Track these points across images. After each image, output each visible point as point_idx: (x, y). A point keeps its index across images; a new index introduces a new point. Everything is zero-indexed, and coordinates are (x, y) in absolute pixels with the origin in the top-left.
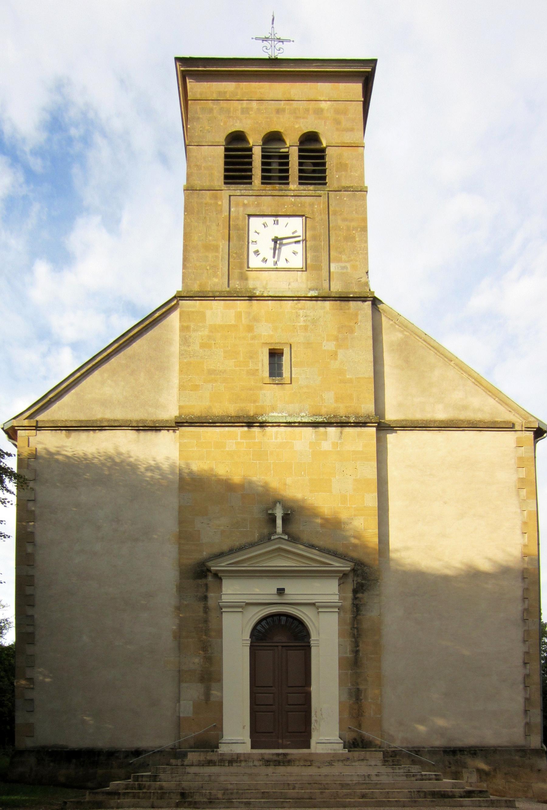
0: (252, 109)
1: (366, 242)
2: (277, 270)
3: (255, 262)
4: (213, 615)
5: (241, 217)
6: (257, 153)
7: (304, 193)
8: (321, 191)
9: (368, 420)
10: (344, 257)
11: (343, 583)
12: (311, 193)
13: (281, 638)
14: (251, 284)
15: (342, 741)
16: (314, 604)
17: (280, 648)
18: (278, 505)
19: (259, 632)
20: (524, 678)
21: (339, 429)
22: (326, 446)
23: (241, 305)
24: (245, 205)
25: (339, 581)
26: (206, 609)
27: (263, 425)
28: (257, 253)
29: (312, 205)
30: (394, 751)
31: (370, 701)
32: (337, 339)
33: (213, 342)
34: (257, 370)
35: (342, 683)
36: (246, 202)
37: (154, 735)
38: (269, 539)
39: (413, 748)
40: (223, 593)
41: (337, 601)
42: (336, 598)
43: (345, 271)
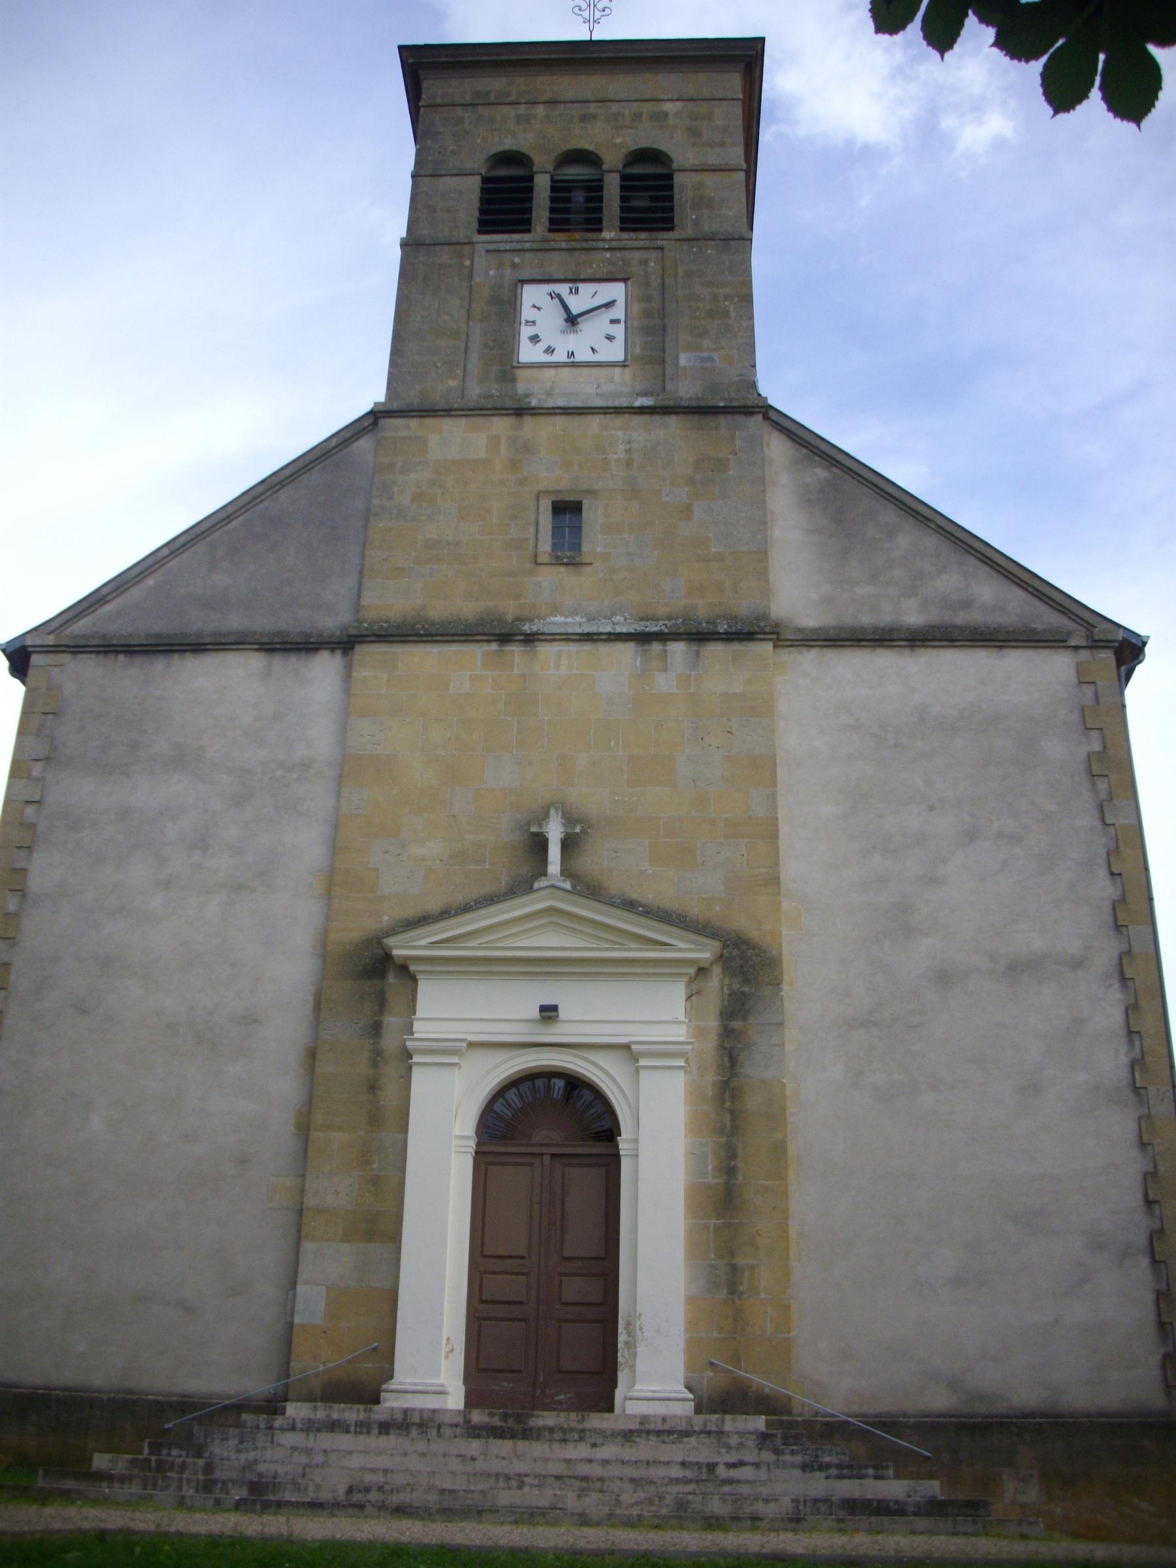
0: (535, 116)
1: (751, 318)
2: (574, 365)
3: (528, 353)
4: (390, 1071)
5: (506, 285)
6: (542, 183)
7: (630, 244)
8: (664, 239)
9: (756, 629)
10: (706, 343)
11: (699, 992)
12: (641, 244)
13: (548, 1135)
14: (521, 387)
15: (691, 1396)
16: (626, 1047)
17: (547, 1159)
18: (553, 813)
19: (499, 1117)
20: (1151, 1239)
21: (694, 647)
22: (664, 683)
23: (501, 426)
24: (514, 266)
25: (687, 987)
26: (377, 1058)
27: (530, 639)
28: (535, 339)
29: (644, 263)
30: (828, 1424)
31: (762, 1296)
32: (691, 482)
33: (439, 492)
34: (526, 539)
35: (694, 1250)
36: (517, 260)
37: (222, 1366)
38: (530, 889)
39: (876, 1416)
40: (419, 1014)
41: (682, 1039)
42: (679, 1034)
43: (709, 364)
